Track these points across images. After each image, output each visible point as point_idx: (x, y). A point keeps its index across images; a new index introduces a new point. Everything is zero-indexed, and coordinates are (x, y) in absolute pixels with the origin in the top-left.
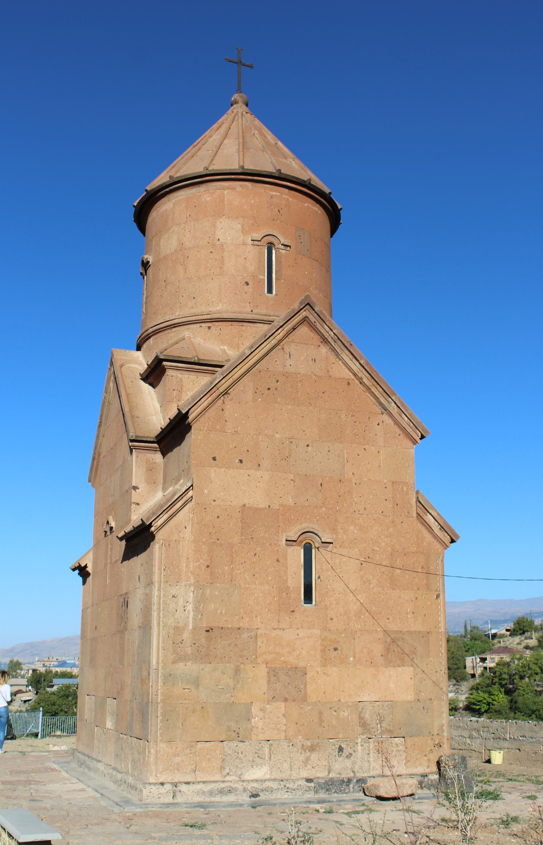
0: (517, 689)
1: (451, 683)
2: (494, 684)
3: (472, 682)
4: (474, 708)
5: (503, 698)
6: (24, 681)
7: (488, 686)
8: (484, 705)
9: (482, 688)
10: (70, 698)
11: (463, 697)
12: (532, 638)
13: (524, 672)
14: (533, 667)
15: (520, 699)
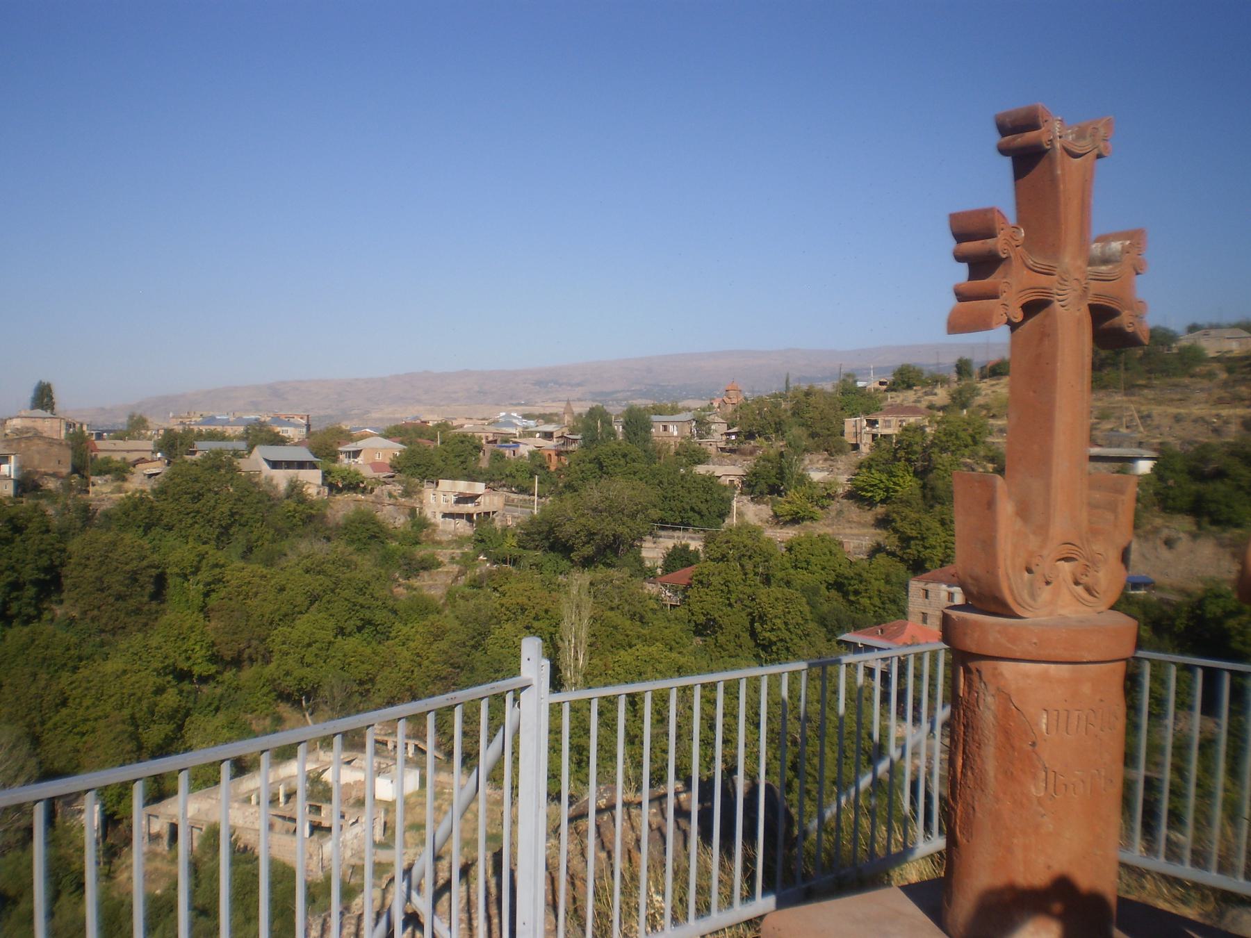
0: (936, 468)
1: (820, 457)
2: (899, 460)
3: (854, 458)
4: (864, 496)
5: (910, 481)
6: (149, 445)
7: (887, 462)
8: (880, 491)
9: (877, 465)
10: (223, 471)
11: (843, 479)
12: (935, 394)
13: (948, 441)
14: (962, 434)
15: (940, 484)
